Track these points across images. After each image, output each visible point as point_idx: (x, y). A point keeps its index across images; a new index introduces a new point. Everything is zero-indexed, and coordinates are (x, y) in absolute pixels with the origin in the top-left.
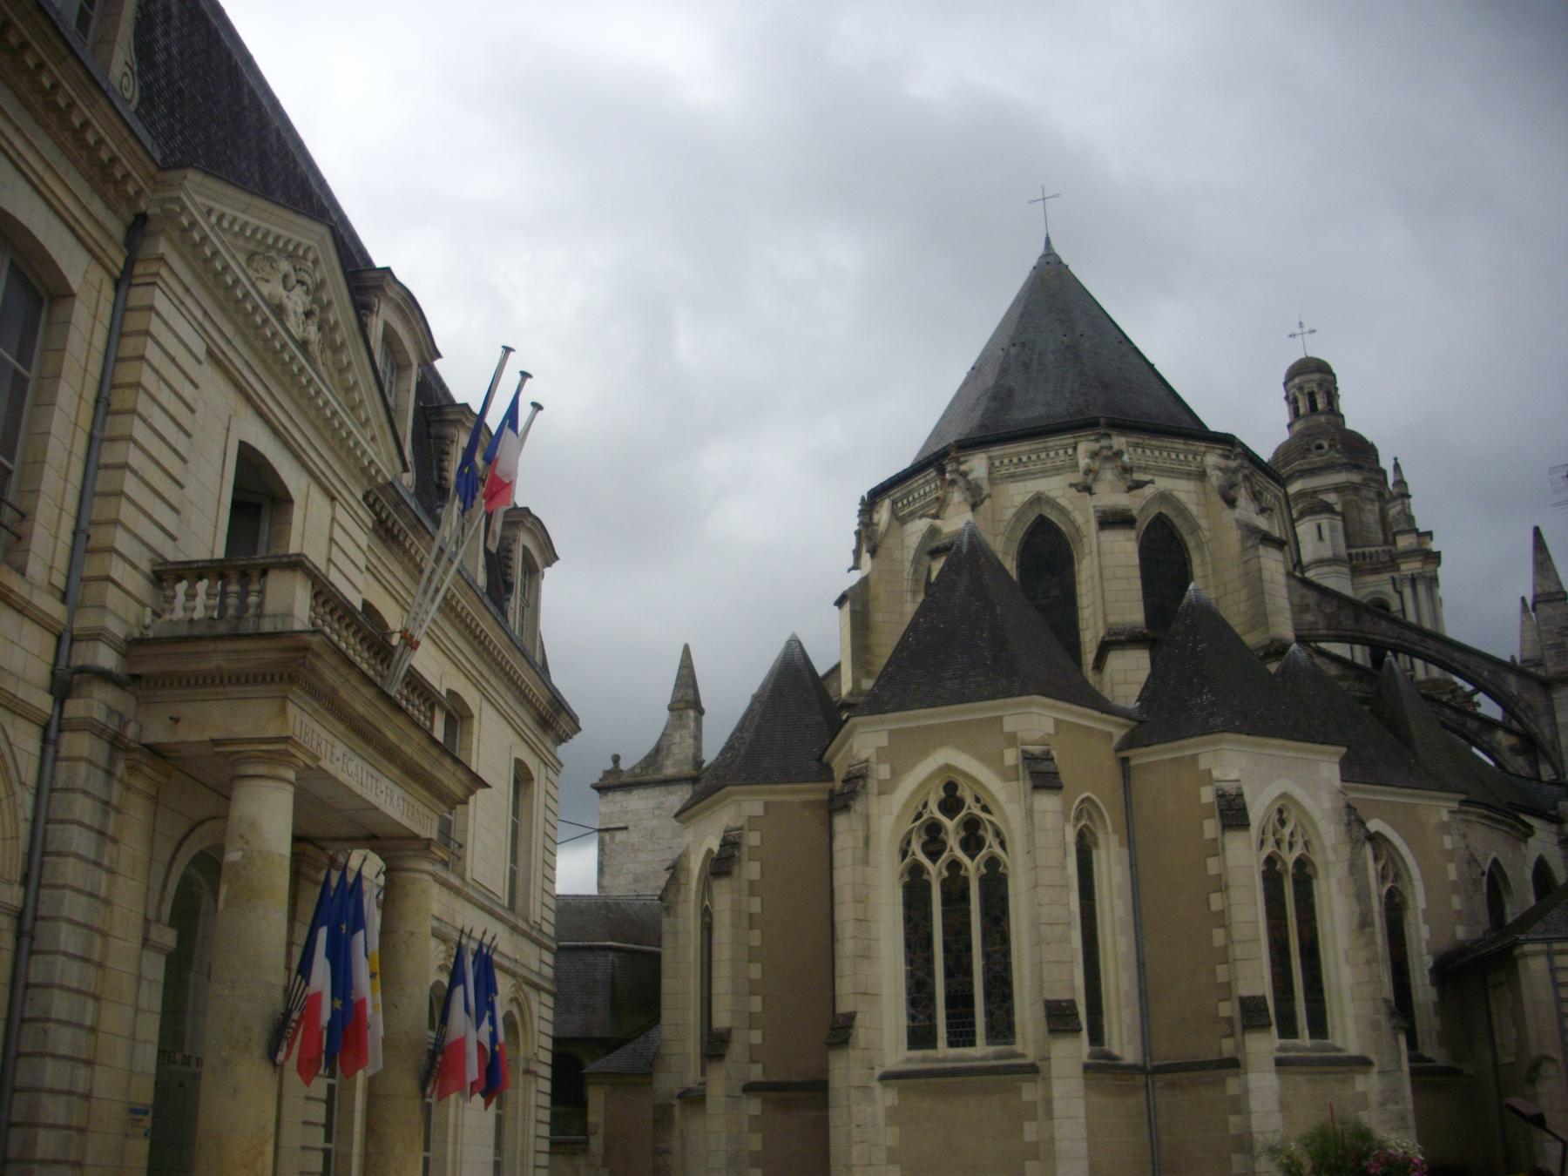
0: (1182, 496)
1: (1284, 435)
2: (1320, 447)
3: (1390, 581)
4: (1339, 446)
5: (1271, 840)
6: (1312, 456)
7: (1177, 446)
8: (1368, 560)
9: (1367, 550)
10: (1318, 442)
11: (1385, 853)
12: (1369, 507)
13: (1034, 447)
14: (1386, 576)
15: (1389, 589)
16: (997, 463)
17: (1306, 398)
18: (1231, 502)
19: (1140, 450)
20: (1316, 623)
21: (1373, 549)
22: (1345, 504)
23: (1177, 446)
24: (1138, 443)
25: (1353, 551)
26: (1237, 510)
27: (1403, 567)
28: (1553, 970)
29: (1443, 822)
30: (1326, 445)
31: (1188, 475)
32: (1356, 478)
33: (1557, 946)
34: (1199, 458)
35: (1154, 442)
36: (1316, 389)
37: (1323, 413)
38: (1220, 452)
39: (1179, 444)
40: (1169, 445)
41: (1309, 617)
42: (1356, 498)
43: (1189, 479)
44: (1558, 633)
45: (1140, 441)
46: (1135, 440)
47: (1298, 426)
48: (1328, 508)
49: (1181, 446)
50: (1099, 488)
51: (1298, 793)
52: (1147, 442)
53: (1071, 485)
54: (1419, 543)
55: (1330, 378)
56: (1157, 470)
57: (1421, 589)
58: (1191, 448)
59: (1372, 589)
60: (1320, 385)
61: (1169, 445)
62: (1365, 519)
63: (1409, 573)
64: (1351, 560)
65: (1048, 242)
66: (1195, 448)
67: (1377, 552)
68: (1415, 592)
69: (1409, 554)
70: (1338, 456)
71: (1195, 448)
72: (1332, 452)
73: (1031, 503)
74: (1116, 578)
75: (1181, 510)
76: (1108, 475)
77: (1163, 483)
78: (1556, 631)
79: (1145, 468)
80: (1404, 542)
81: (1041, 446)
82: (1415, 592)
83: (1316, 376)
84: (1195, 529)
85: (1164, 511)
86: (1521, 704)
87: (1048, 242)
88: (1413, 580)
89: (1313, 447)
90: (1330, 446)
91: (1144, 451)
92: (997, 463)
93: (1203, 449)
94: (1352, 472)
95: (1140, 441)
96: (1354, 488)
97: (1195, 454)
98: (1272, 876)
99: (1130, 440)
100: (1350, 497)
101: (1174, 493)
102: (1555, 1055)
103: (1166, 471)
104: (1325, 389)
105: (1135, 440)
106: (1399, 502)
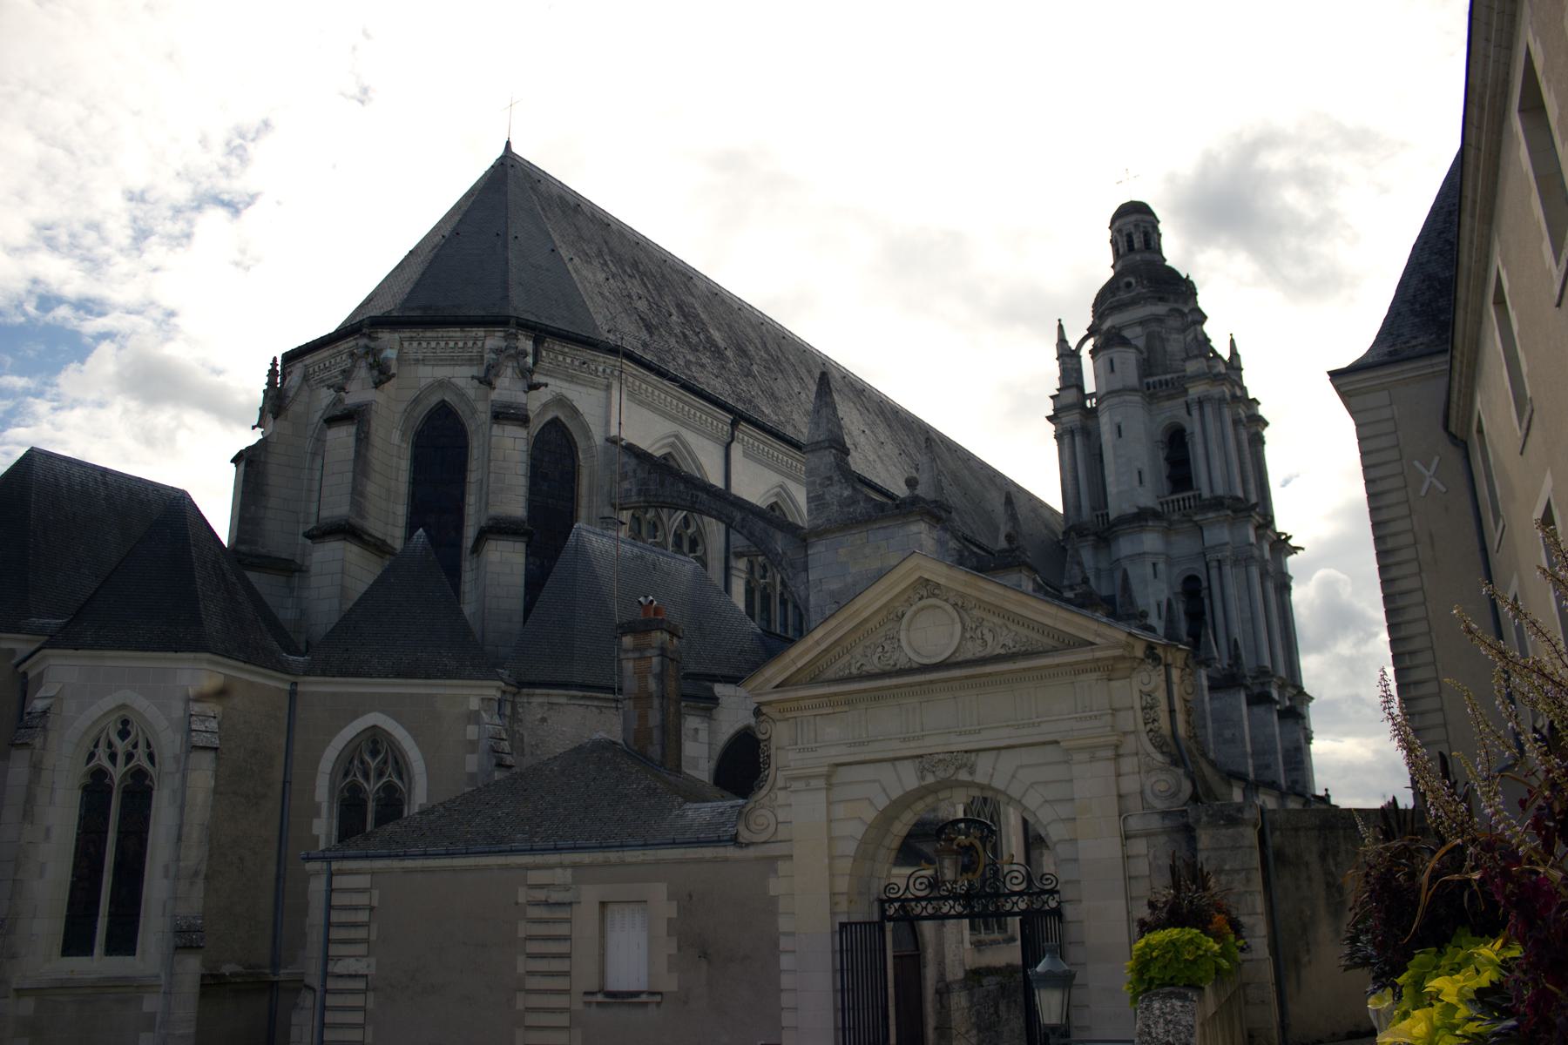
0: (461, 383)
1: (1110, 274)
2: (1129, 285)
3: (1185, 406)
4: (1145, 282)
5: (102, 752)
6: (1121, 293)
7: (453, 334)
8: (1164, 387)
9: (1163, 378)
10: (1126, 280)
11: (385, 745)
12: (1176, 336)
13: (331, 351)
14: (1182, 400)
15: (1183, 412)
16: (311, 369)
17: (1125, 239)
18: (490, 385)
19: (415, 344)
20: (631, 490)
21: (1168, 377)
22: (1150, 337)
23: (453, 334)
24: (412, 337)
25: (1151, 380)
26: (496, 391)
27: (1191, 391)
28: (330, 891)
29: (471, 712)
30: (1133, 281)
31: (470, 361)
32: (1160, 309)
33: (335, 866)
34: (479, 343)
35: (429, 334)
36: (1133, 230)
37: (1140, 251)
38: (502, 334)
39: (456, 333)
40: (445, 335)
41: (626, 485)
42: (1159, 329)
43: (471, 365)
44: (820, 484)
45: (414, 335)
46: (408, 335)
47: (1118, 267)
48: (1126, 343)
49: (459, 334)
50: (353, 387)
51: (141, 703)
52: (421, 335)
53: (473, 377)
54: (1209, 367)
55: (1146, 217)
56: (435, 360)
57: (1208, 410)
58: (470, 334)
59: (1168, 414)
60: (1136, 226)
61: (445, 335)
62: (1169, 348)
63: (1195, 397)
64: (1149, 389)
65: (508, 144)
66: (474, 334)
67: (1172, 379)
68: (1202, 415)
69: (1197, 377)
70: (1144, 291)
71: (474, 334)
72: (1139, 287)
73: (335, 404)
74: (333, 474)
75: (460, 394)
76: (363, 373)
77: (442, 372)
78: (818, 482)
79: (423, 360)
80: (1192, 367)
81: (335, 351)
82: (1202, 415)
83: (1133, 218)
84: (474, 411)
85: (446, 399)
86: (784, 563)
87: (508, 144)
88: (1201, 403)
89: (1122, 284)
90: (1137, 282)
91: (420, 344)
92: (311, 369)
93: (483, 334)
94: (1157, 305)
95: (414, 335)
96: (1158, 319)
97: (476, 340)
98: (95, 790)
99: (403, 335)
100: (1154, 327)
101: (453, 380)
102: (316, 987)
103: (446, 360)
104: (1142, 229)
105: (408, 335)
106: (1192, 328)
